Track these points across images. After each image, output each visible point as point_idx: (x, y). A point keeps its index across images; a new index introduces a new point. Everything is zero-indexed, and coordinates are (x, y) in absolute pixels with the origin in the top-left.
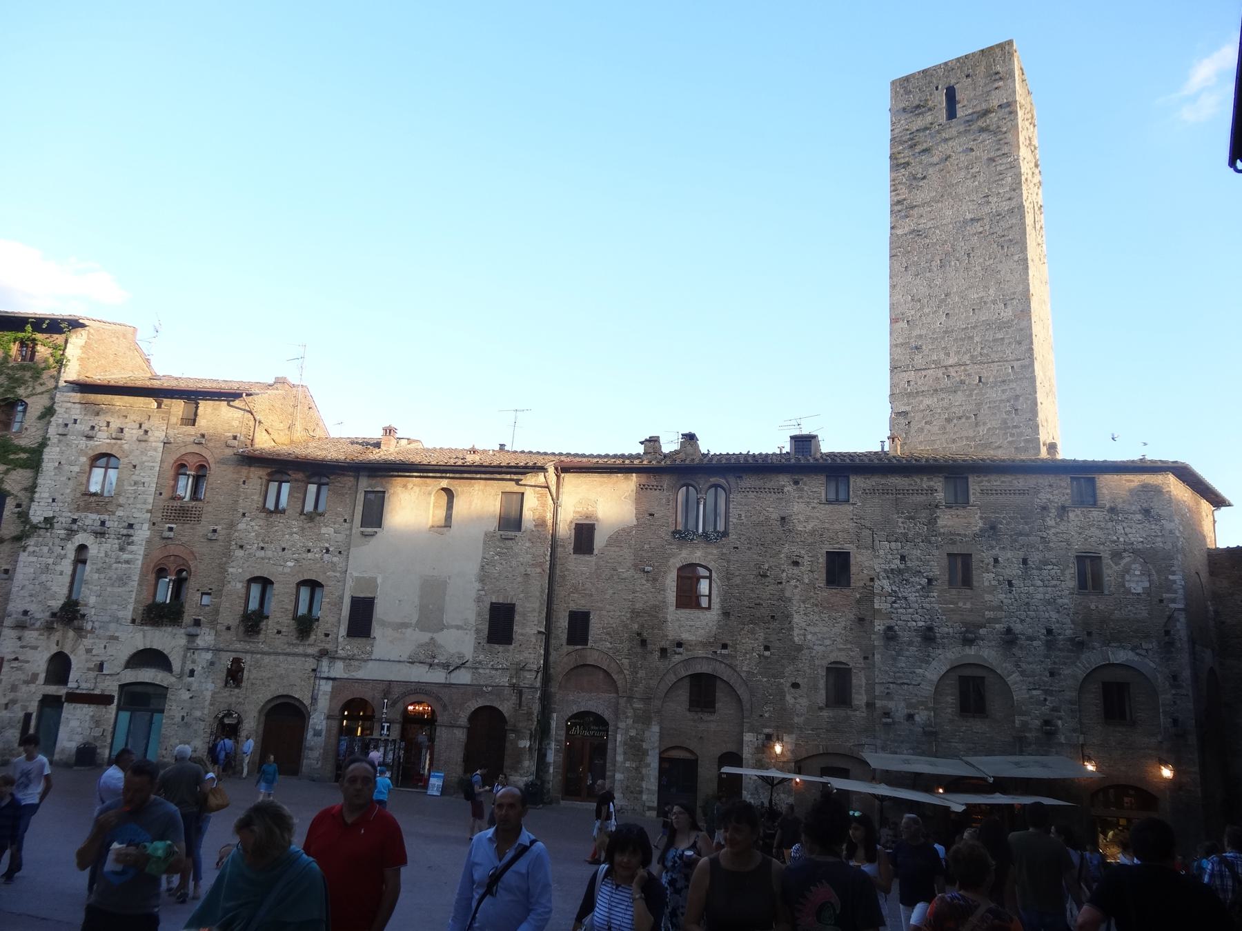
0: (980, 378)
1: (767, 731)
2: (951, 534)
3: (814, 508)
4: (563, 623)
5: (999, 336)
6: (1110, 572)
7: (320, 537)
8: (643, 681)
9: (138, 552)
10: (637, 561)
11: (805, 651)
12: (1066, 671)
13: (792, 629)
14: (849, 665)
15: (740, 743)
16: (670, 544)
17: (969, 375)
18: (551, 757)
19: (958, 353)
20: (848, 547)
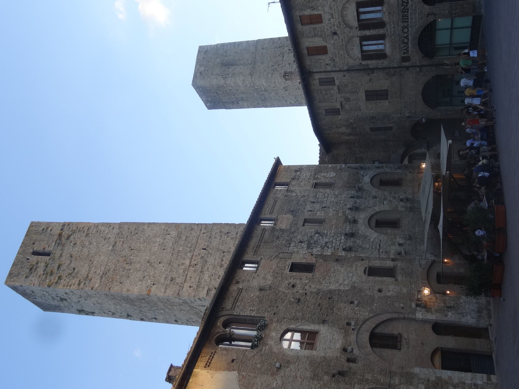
0: (203, 249)
1: (413, 306)
2: (291, 224)
3: (258, 276)
5: (184, 238)
8: (375, 376)
10: (270, 373)
11: (356, 285)
13: (339, 290)
14: (366, 268)
15: (424, 321)
16: (261, 350)
17: (199, 254)
19: (184, 259)
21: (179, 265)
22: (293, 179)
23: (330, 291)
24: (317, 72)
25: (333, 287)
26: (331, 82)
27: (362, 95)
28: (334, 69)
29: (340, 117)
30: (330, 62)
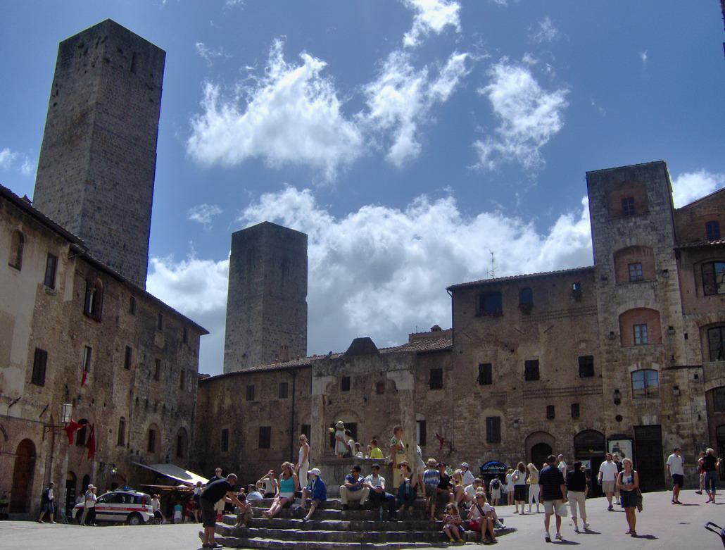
1: (101, 460)
13: (112, 393)
15: (91, 468)
17: (121, 240)
21: (111, 217)
22: (189, 348)
23: (112, 385)
24: (294, 382)
26: (283, 394)
27: (266, 424)
28: (296, 399)
29: (244, 400)
30: (303, 395)
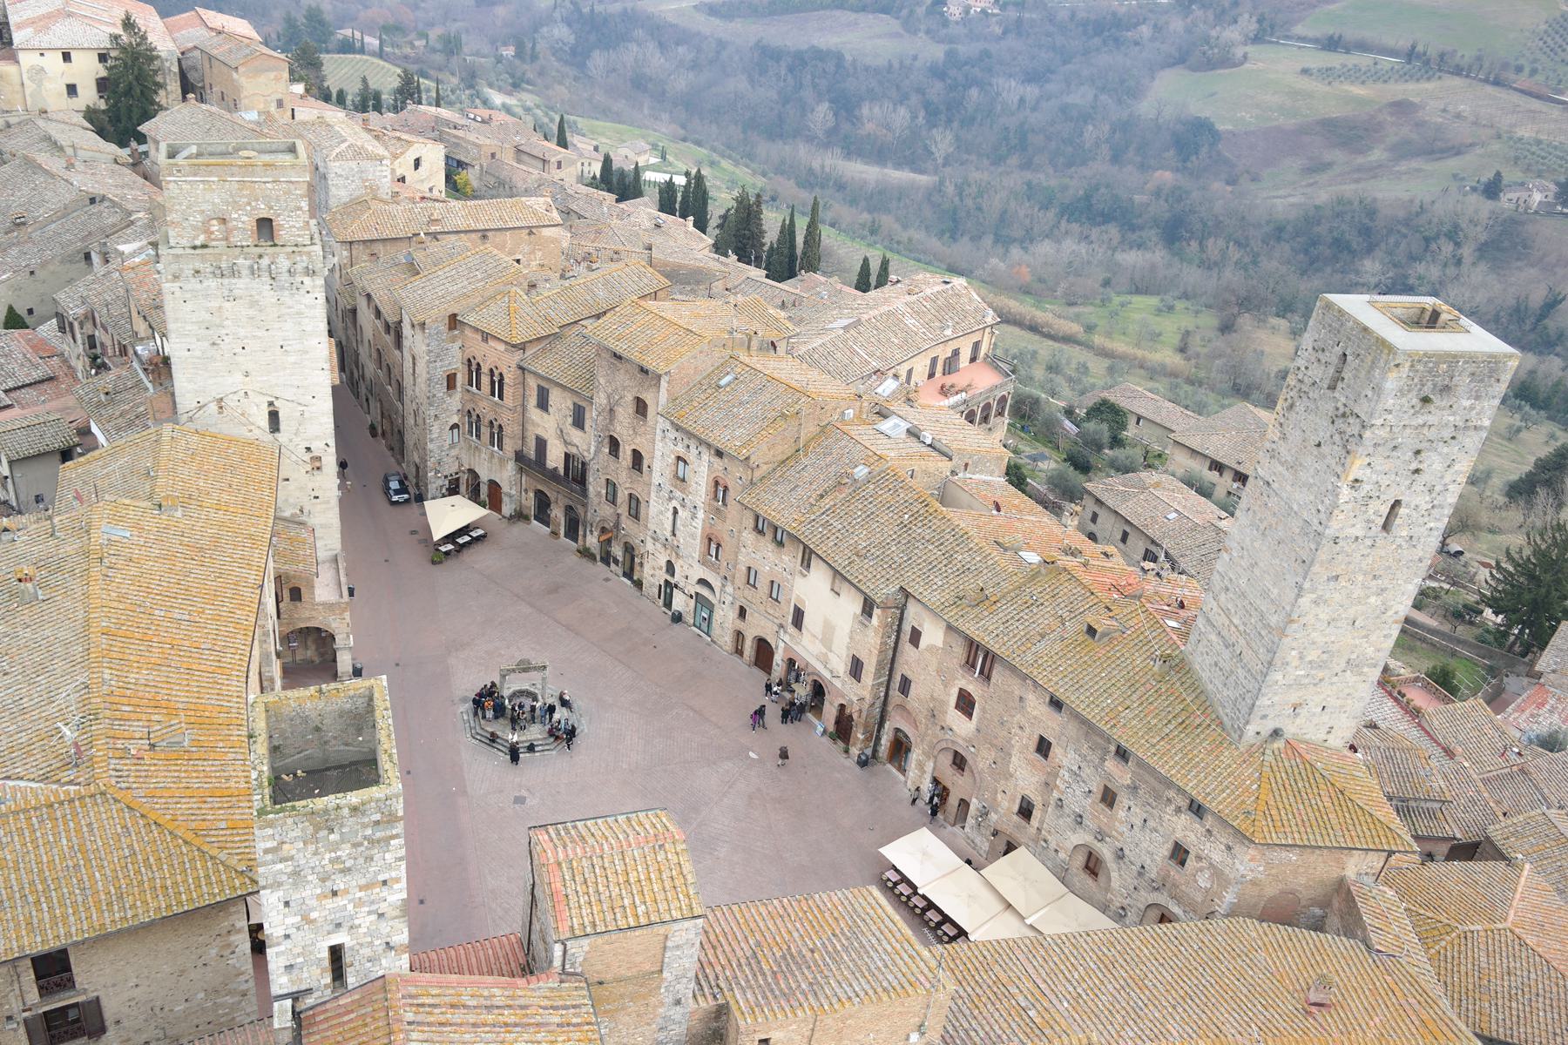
4: (897, 678)
6: (1191, 862)
7: (781, 560)
9: (699, 523)
12: (1143, 893)
18: (883, 741)
20: (1051, 740)
25: (1013, 759)
